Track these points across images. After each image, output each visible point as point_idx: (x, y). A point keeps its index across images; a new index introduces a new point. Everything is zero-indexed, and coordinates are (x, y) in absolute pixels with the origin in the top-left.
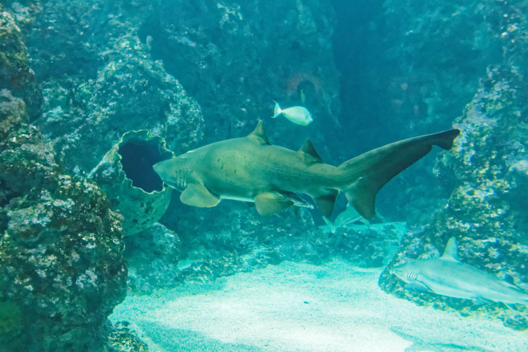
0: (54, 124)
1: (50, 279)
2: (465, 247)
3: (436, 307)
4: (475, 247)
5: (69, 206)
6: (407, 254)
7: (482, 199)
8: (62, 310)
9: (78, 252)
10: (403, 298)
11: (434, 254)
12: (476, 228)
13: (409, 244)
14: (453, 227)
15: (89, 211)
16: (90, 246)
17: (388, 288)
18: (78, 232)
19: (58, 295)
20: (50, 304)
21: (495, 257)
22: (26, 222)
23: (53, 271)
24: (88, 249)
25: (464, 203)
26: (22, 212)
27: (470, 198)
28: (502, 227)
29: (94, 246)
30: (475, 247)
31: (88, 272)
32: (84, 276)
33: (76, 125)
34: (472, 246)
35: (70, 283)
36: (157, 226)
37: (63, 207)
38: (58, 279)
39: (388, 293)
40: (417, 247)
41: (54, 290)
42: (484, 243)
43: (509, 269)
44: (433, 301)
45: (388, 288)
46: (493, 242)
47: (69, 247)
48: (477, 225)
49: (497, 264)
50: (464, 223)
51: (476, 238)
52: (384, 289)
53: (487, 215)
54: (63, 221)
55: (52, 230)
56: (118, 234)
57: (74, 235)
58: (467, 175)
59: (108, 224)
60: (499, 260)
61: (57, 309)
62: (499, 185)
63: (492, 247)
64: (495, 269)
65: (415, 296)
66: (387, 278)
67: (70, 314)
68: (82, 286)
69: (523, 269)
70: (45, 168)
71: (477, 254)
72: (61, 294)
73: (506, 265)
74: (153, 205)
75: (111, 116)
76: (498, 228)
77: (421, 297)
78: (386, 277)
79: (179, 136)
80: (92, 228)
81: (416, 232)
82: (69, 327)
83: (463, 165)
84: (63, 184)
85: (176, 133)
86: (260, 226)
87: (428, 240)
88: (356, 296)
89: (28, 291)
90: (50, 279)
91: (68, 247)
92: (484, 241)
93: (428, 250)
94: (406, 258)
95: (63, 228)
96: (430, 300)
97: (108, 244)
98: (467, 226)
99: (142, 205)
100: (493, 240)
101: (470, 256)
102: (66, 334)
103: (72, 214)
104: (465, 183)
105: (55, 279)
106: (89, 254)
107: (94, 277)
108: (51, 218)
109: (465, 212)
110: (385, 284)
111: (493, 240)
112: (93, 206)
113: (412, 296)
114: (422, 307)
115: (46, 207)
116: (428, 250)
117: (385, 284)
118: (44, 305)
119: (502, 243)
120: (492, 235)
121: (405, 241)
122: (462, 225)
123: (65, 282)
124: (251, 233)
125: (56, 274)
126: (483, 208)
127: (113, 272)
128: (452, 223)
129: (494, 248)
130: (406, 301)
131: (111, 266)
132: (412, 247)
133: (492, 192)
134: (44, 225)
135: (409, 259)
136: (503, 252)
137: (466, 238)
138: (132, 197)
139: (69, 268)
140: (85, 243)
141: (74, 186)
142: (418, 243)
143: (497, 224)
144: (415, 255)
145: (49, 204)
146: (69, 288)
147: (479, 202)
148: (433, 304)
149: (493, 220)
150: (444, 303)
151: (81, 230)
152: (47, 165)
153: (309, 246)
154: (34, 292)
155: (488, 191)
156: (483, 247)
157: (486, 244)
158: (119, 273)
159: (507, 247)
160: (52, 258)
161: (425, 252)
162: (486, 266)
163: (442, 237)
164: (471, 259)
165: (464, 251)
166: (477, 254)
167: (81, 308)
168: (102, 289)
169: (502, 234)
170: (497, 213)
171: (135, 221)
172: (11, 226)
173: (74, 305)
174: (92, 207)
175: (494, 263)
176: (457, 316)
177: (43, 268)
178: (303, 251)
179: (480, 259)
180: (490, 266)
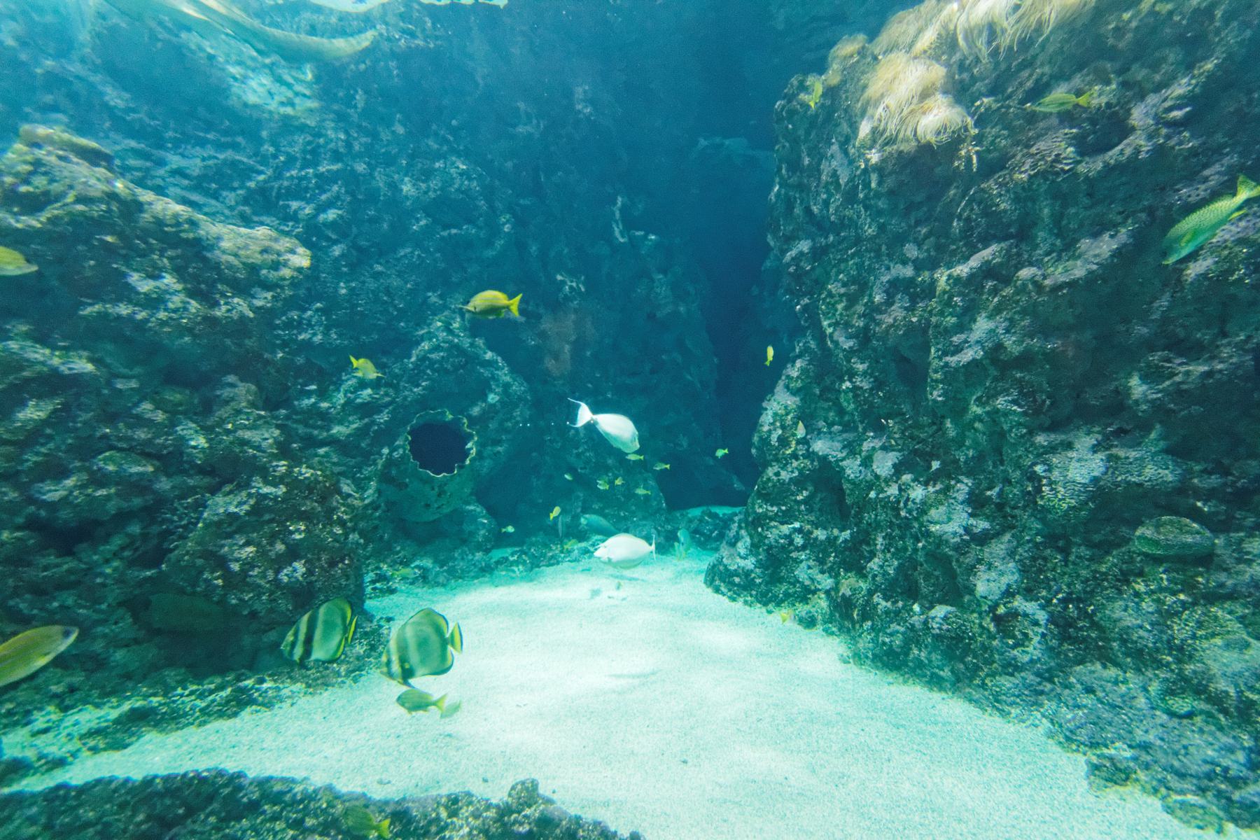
0: (363, 405)
5: (280, 493)
16: (297, 536)
20: (241, 600)
24: (294, 540)
29: (303, 536)
31: (296, 564)
32: (290, 569)
33: (386, 405)
37: (271, 494)
38: (256, 572)
47: (273, 537)
54: (269, 510)
55: (253, 518)
67: (272, 610)
68: (286, 579)
70: (258, 454)
75: (422, 396)
79: (501, 415)
80: (306, 517)
84: (275, 471)
85: (497, 412)
89: (218, 586)
95: (267, 517)
102: (270, 633)
103: (282, 502)
105: (251, 573)
108: (252, 506)
123: (264, 577)
134: (242, 513)
140: (292, 533)
141: (292, 472)
146: (269, 582)
151: (290, 518)
152: (264, 452)
154: (223, 586)
158: (340, 565)
174: (310, 494)
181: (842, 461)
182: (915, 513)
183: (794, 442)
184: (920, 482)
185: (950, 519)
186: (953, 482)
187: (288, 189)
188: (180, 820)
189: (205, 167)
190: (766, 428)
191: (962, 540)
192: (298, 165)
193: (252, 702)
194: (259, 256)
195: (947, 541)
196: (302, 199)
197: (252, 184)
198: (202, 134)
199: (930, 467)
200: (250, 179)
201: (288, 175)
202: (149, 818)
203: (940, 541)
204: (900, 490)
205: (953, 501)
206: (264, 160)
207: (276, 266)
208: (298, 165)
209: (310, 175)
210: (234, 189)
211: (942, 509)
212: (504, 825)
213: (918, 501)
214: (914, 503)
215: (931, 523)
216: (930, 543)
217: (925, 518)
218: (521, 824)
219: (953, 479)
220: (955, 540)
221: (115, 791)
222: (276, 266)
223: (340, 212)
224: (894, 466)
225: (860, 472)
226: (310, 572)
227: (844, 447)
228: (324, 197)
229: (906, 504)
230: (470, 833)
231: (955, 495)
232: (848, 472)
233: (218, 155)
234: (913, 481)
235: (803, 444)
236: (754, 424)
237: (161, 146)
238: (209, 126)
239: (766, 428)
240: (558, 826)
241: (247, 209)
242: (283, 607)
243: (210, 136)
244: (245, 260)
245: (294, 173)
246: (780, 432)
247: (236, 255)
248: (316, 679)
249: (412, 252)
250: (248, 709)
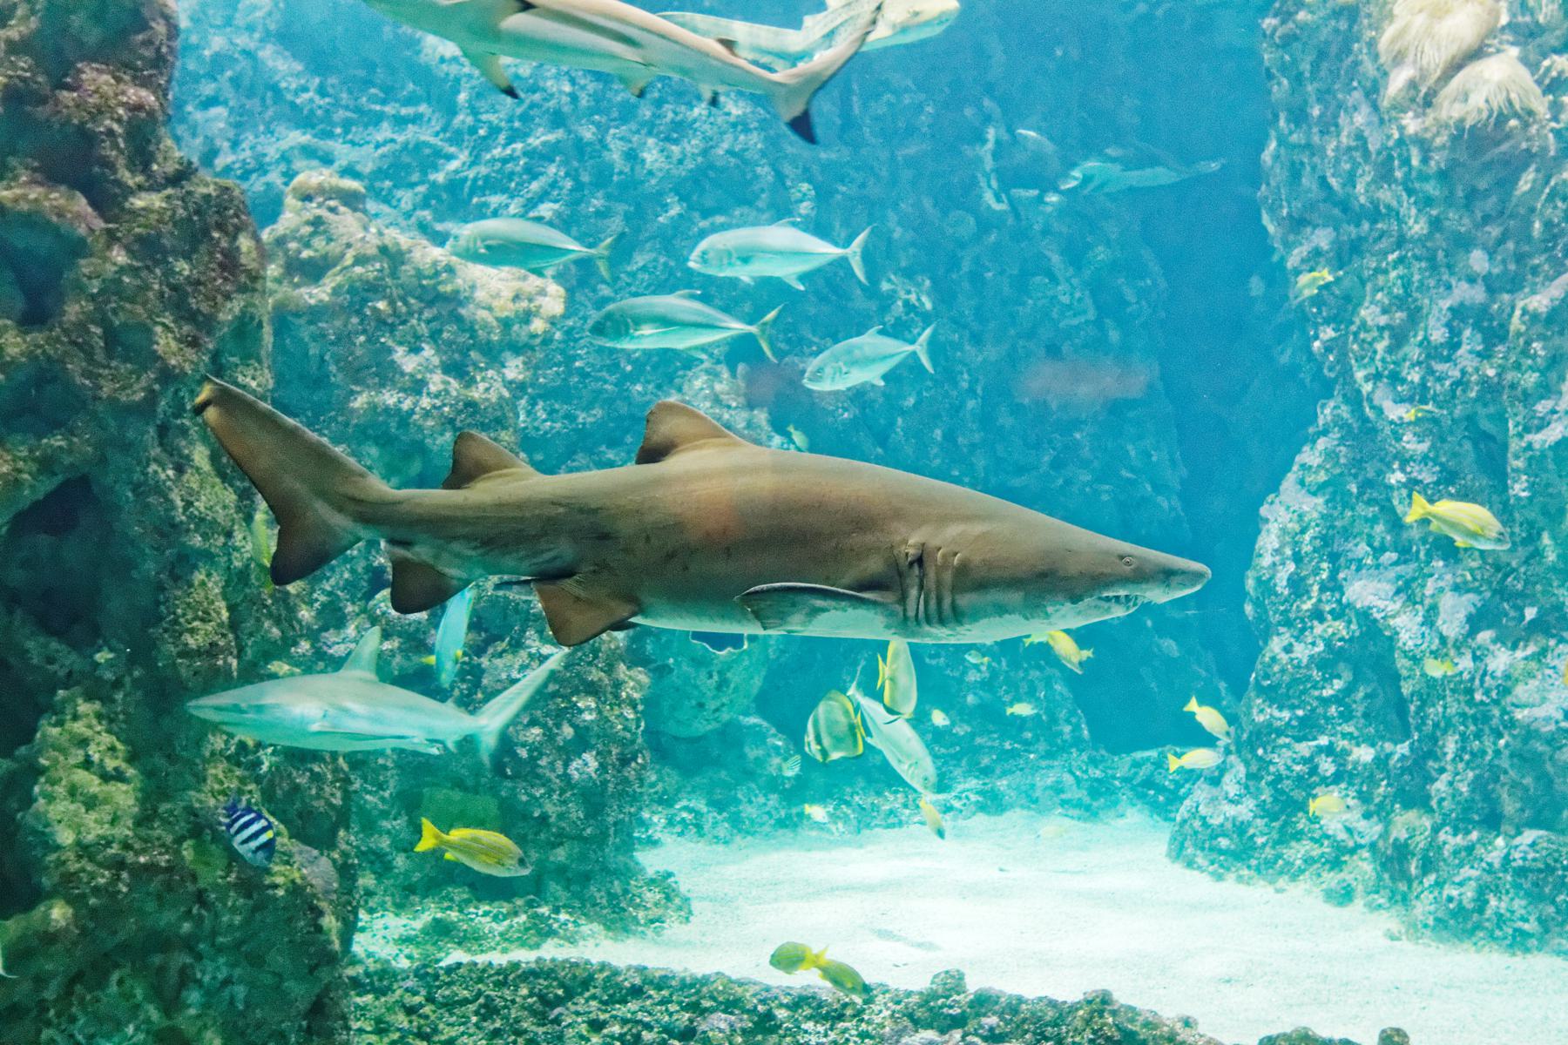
1: (533, 760)
7: (1305, 661)
8: (551, 809)
9: (572, 725)
12: (1298, 718)
15: (590, 664)
16: (588, 717)
18: (572, 694)
19: (543, 785)
22: (504, 676)
23: (536, 749)
25: (1276, 668)
26: (498, 662)
27: (1284, 657)
28: (1341, 714)
31: (587, 756)
35: (560, 771)
36: (756, 725)
38: (543, 762)
41: (538, 776)
47: (560, 716)
48: (1300, 713)
50: (1280, 708)
51: (1299, 740)
53: (1316, 693)
56: (633, 704)
57: (566, 698)
58: (1282, 613)
59: (618, 685)
61: (540, 806)
62: (1330, 631)
67: (561, 816)
68: (576, 776)
72: (546, 783)
74: (729, 675)
80: (593, 689)
82: (560, 839)
83: (1277, 595)
86: (973, 735)
90: (533, 760)
91: (558, 716)
97: (617, 717)
98: (1286, 714)
99: (711, 676)
104: (1281, 630)
106: (587, 729)
107: (593, 764)
109: (1279, 685)
112: (595, 657)
115: (530, 655)
118: (524, 798)
122: (1277, 713)
123: (553, 770)
124: (952, 751)
125: (541, 754)
126: (1309, 678)
127: (625, 761)
128: (1261, 711)
131: (622, 753)
133: (1320, 647)
137: (1283, 740)
138: (693, 660)
139: (559, 749)
140: (581, 711)
143: (1333, 710)
145: (533, 651)
147: (1299, 667)
151: (576, 692)
155: (1314, 644)
159: (1349, 753)
160: (536, 731)
164: (1288, 778)
166: (1298, 768)
167: (576, 812)
168: (604, 783)
171: (701, 705)
172: (485, 681)
173: (564, 802)
177: (524, 745)
178: (1058, 789)
181: (1394, 617)
182: (1494, 694)
183: (1316, 588)
184: (1504, 644)
185: (1544, 700)
186: (1552, 642)
187: (487, 178)
188: (559, 1001)
189: (384, 156)
190: (1267, 561)
191: (1559, 729)
192: (502, 138)
193: (551, 933)
194: (511, 305)
195: (1537, 731)
196: (504, 190)
197: (440, 177)
198: (378, 108)
199: (1522, 616)
200: (436, 168)
201: (488, 156)
202: (531, 995)
203: (1530, 733)
204: (1475, 658)
205: (1548, 672)
206: (457, 139)
207: (527, 317)
208: (502, 138)
209: (518, 153)
210: (413, 185)
211: (1533, 683)
212: (931, 1009)
213: (1499, 674)
214: (1493, 678)
215: (1516, 706)
216: (1514, 737)
217: (1509, 699)
218: (951, 1007)
219: (1553, 636)
220: (1548, 728)
221: (484, 971)
222: (527, 317)
223: (556, 206)
224: (1470, 619)
225: (1423, 635)
226: (603, 767)
227: (1398, 592)
228: (535, 186)
229: (1482, 682)
230: (892, 1016)
231: (1556, 662)
232: (1404, 636)
233: (395, 136)
234: (1494, 641)
235: (1332, 590)
236: (1247, 553)
237: (329, 135)
238: (389, 94)
239: (1267, 561)
240: (997, 1003)
241: (426, 214)
242: (573, 816)
243: (389, 109)
244: (499, 314)
245: (497, 152)
246: (1291, 567)
247: (490, 309)
248: (613, 922)
249: (655, 260)
250: (549, 941)
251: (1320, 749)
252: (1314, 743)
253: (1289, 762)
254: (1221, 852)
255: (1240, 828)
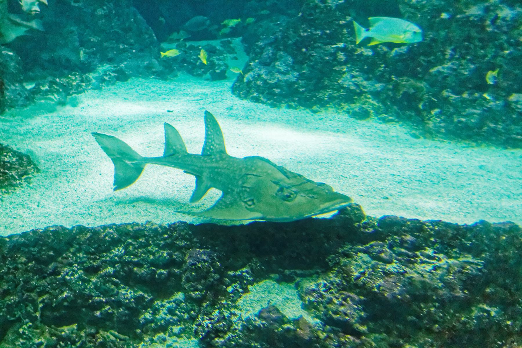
2: (316, 52)
3: (289, 107)
4: (326, 52)
6: (260, 63)
10: (259, 102)
11: (286, 61)
13: (261, 53)
14: (305, 34)
17: (243, 94)
21: (342, 60)
30: (326, 52)
34: (322, 51)
39: (242, 99)
40: (270, 55)
42: (333, 48)
43: (353, 70)
44: (286, 102)
45: (243, 94)
46: (342, 47)
49: (343, 67)
50: (316, 30)
52: (239, 96)
60: (345, 63)
63: (340, 53)
64: (342, 71)
65: (269, 99)
66: (241, 86)
69: (366, 69)
71: (327, 58)
73: (351, 67)
76: (346, 34)
77: (275, 100)
78: (239, 86)
81: (267, 42)
87: (281, 47)
88: (214, 104)
92: (333, 46)
93: (281, 57)
94: (259, 66)
96: (283, 102)
98: (319, 32)
100: (341, 45)
101: (321, 61)
110: (239, 92)
111: (341, 45)
113: (266, 100)
114: (276, 108)
116: (281, 57)
117: (239, 92)
119: (349, 47)
120: (340, 41)
121: (256, 51)
128: (305, 31)
129: (342, 52)
130: (261, 104)
132: (265, 55)
135: (262, 67)
136: (349, 56)
142: (271, 51)
144: (268, 63)
148: (286, 105)
149: (342, 27)
150: (296, 103)
153: (155, 61)
156: (333, 52)
157: (335, 49)
161: (278, 59)
162: (334, 69)
163: (295, 44)
164: (321, 63)
165: (314, 56)
169: (349, 39)
170: (345, 20)
175: (341, 65)
176: (307, 113)
179: (329, 62)
180: (337, 68)
251: (338, 49)
252: (334, 46)
253: (322, 55)
254: (275, 94)
255: (290, 85)
